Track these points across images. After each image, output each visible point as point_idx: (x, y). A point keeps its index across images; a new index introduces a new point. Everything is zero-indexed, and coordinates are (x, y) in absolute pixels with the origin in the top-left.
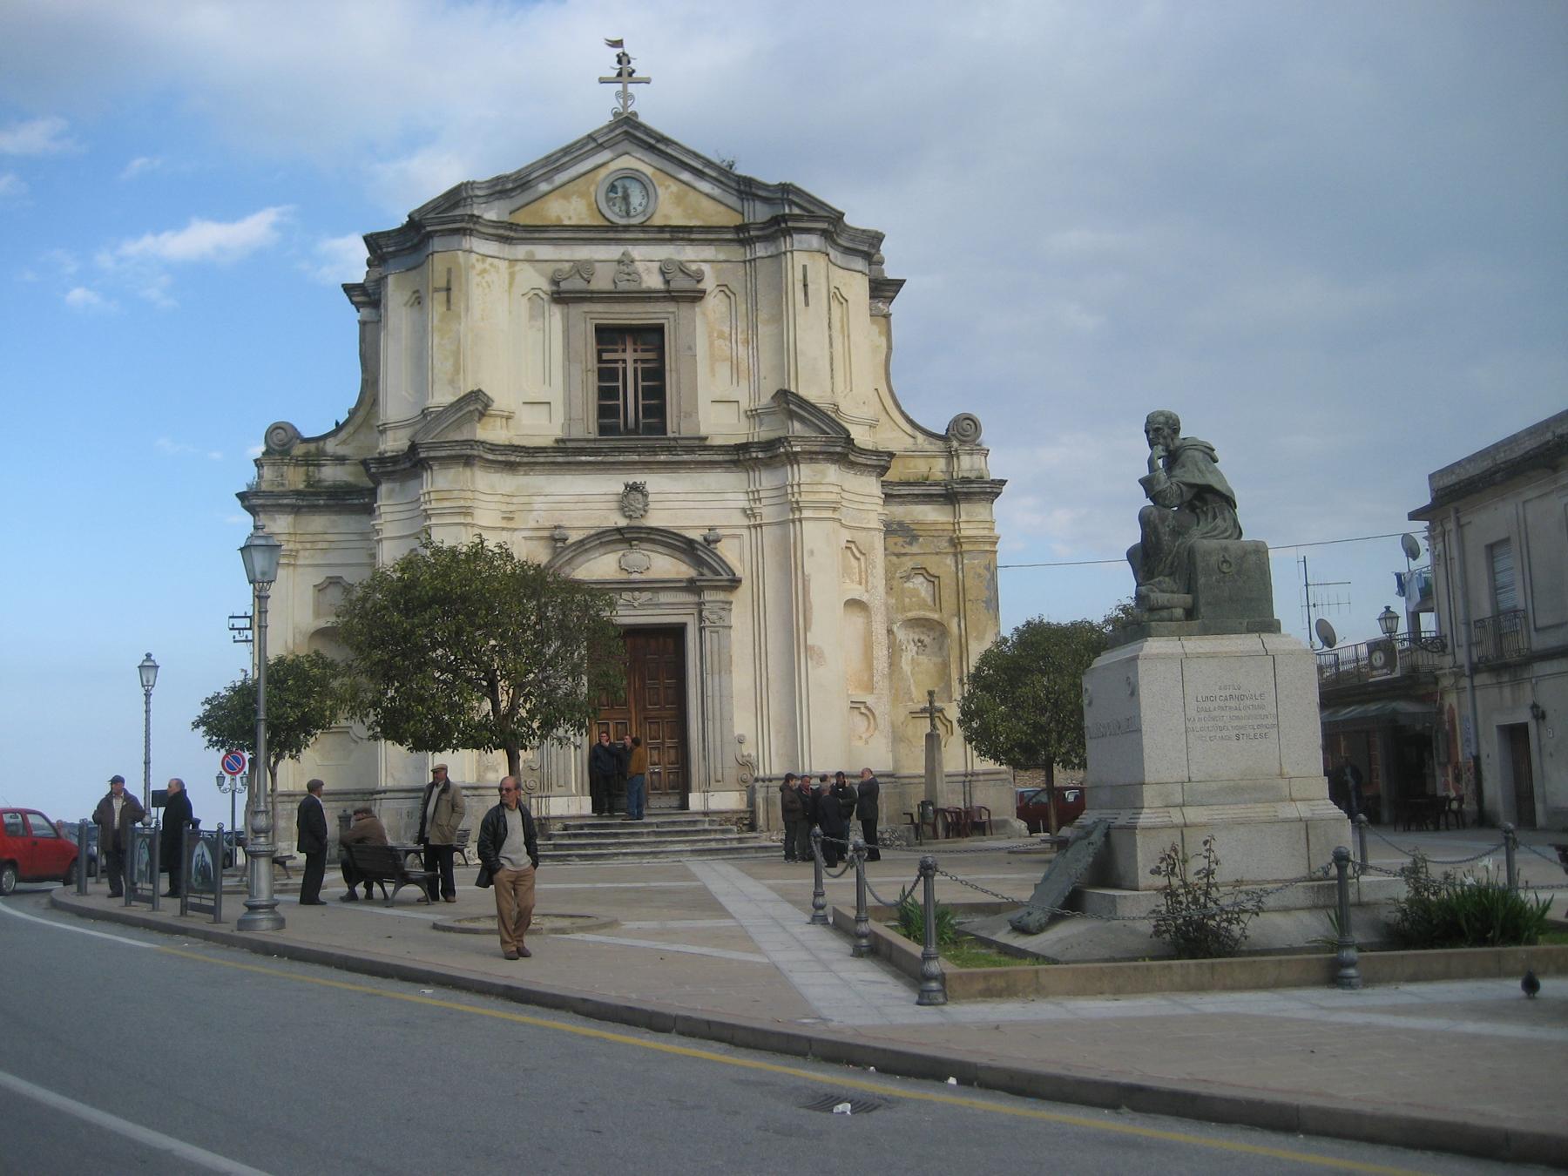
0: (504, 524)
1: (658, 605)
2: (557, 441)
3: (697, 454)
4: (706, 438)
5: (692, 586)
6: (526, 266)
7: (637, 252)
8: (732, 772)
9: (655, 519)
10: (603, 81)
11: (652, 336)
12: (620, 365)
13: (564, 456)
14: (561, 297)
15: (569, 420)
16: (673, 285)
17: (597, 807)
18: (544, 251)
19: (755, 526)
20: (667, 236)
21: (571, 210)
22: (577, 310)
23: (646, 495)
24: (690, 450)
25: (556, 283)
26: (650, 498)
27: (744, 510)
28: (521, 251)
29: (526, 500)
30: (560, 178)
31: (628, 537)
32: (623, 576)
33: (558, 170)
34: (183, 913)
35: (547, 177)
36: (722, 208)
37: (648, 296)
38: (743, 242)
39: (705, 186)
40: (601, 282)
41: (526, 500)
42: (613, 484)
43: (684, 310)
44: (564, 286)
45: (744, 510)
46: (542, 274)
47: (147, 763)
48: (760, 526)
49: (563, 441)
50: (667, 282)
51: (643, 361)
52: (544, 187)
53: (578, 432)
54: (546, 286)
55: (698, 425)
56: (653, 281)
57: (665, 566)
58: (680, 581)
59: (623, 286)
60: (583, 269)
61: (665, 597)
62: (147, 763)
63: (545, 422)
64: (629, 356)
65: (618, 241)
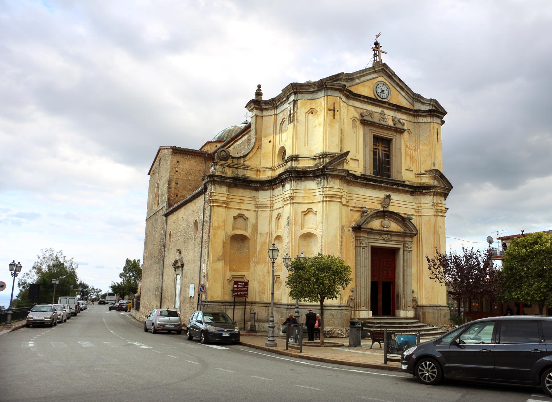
0: (435, 214)
1: (391, 241)
2: (362, 175)
3: (401, 187)
4: (404, 182)
5: (404, 235)
6: (352, 108)
7: (386, 112)
8: (411, 303)
9: (391, 209)
10: (386, 53)
11: (388, 142)
12: (377, 151)
13: (363, 181)
14: (364, 123)
15: (365, 168)
16: (397, 126)
17: (373, 314)
18: (358, 104)
19: (419, 216)
20: (395, 108)
21: (365, 90)
22: (367, 129)
23: (390, 199)
24: (397, 185)
25: (362, 116)
26: (391, 201)
27: (415, 209)
28: (351, 102)
29: (352, 195)
30: (363, 79)
31: (384, 214)
32: (381, 228)
33: (362, 76)
34: (287, 349)
35: (358, 78)
36: (408, 103)
37: (389, 128)
38: (414, 116)
39: (403, 94)
40: (376, 120)
41: (352, 195)
42: (381, 195)
43: (398, 136)
44: (365, 118)
45: (415, 209)
46: (358, 113)
47: (13, 290)
48: (421, 216)
49: (364, 175)
50: (395, 124)
51: (385, 151)
52: (357, 81)
53: (368, 173)
54: (358, 116)
55: (402, 177)
56: (391, 123)
57: (394, 226)
58: (400, 233)
59: (382, 123)
60: (371, 114)
61: (393, 238)
62: (13, 290)
63: (357, 166)
64: (380, 148)
65: (380, 106)
